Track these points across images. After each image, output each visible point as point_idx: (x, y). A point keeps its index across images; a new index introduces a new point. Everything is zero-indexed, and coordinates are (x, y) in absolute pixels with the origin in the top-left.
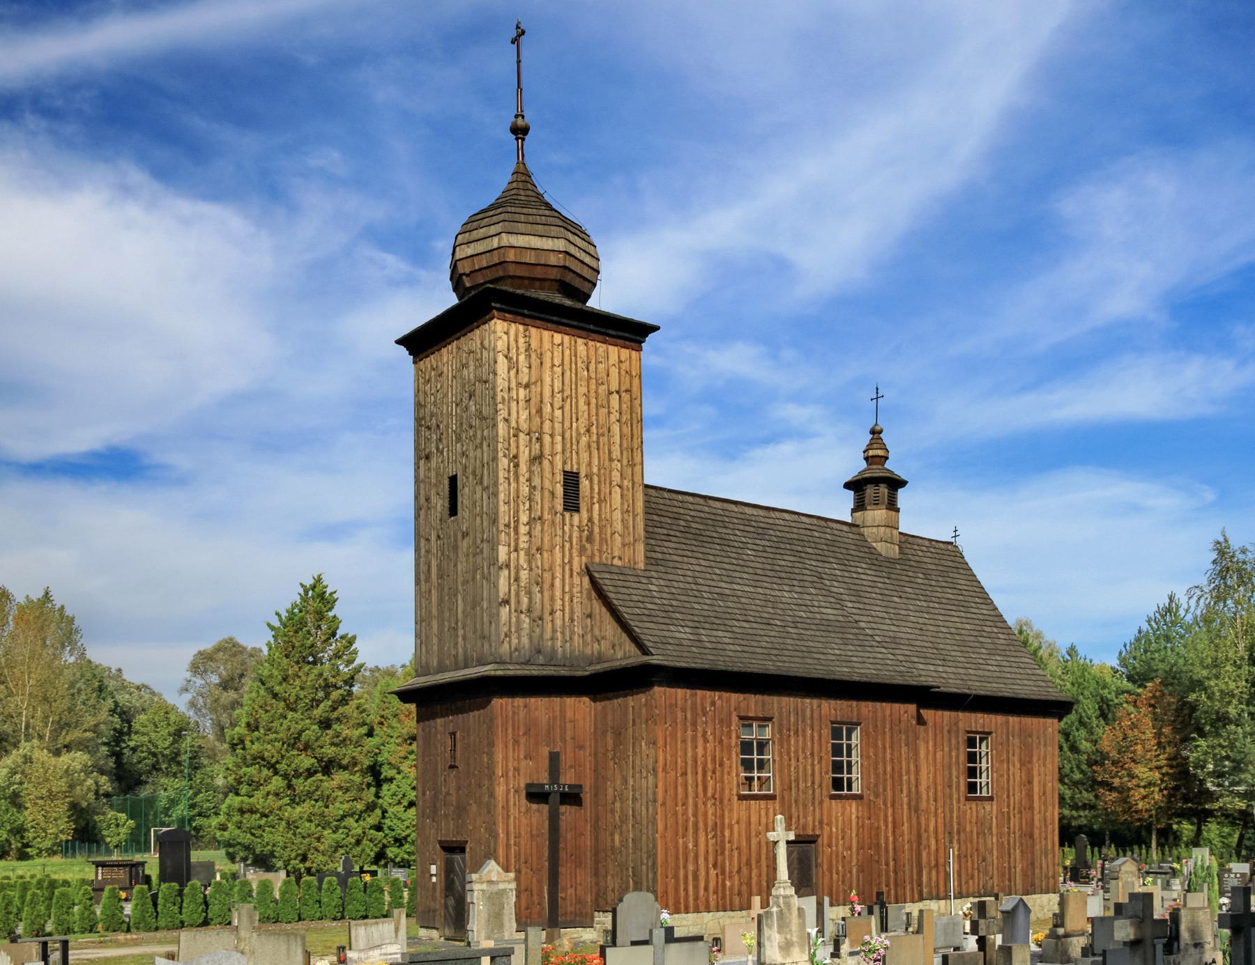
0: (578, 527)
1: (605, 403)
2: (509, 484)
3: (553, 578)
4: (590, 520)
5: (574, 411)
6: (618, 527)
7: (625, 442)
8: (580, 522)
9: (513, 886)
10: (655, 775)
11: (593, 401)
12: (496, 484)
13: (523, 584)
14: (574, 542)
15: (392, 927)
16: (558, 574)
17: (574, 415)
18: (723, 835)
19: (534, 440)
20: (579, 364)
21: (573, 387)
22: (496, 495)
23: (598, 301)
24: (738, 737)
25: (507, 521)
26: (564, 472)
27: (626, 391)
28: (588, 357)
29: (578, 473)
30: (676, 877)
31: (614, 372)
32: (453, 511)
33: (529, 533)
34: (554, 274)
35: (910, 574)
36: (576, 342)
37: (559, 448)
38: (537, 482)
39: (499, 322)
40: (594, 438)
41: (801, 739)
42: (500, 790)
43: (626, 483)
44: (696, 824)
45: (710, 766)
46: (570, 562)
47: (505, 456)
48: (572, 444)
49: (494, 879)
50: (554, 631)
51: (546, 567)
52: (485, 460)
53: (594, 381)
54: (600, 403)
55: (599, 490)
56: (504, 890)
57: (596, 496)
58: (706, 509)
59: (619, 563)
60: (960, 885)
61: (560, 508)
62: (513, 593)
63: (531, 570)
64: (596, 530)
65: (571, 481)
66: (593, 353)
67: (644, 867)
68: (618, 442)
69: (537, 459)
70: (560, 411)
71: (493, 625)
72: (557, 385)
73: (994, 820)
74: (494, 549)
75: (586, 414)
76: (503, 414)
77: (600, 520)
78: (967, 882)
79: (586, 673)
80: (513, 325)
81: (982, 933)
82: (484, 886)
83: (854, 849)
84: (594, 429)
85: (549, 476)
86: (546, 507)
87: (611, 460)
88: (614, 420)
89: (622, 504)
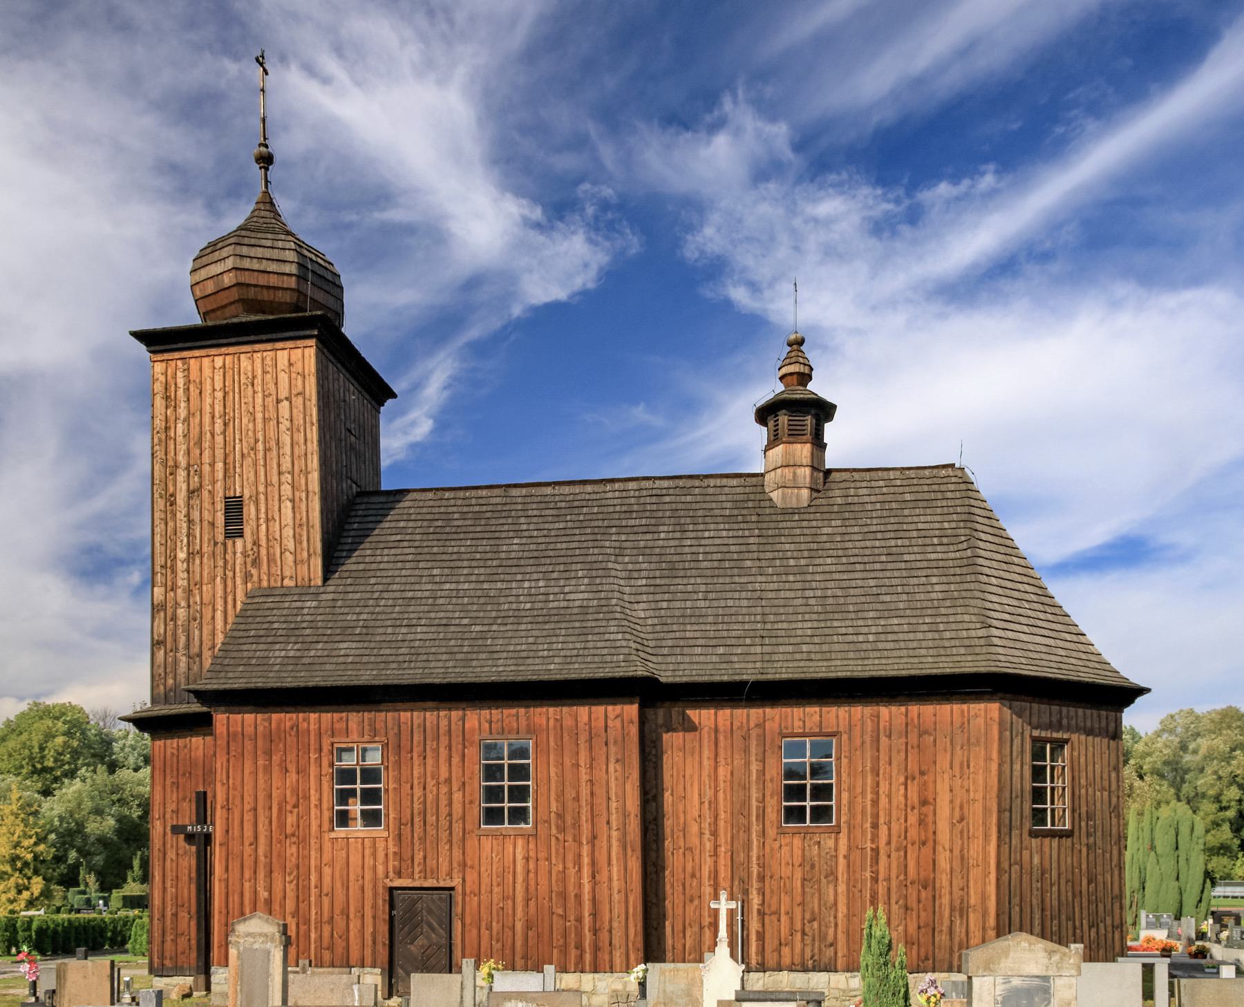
0: (242, 553)
1: (273, 415)
2: (166, 524)
3: (214, 610)
4: (256, 543)
6: (290, 545)
8: (244, 547)
11: (259, 416)
17: (237, 437)
19: (192, 473)
24: (332, 765)
25: (163, 563)
26: (226, 498)
34: (234, 294)
37: (220, 475)
38: (196, 515)
47: (161, 497)
48: (235, 467)
55: (267, 509)
59: (292, 584)
61: (220, 538)
62: (169, 633)
63: (189, 606)
64: (263, 552)
65: (234, 509)
70: (222, 437)
75: (250, 433)
84: (260, 446)
85: (210, 507)
86: (206, 539)
87: (280, 473)
89: (294, 517)
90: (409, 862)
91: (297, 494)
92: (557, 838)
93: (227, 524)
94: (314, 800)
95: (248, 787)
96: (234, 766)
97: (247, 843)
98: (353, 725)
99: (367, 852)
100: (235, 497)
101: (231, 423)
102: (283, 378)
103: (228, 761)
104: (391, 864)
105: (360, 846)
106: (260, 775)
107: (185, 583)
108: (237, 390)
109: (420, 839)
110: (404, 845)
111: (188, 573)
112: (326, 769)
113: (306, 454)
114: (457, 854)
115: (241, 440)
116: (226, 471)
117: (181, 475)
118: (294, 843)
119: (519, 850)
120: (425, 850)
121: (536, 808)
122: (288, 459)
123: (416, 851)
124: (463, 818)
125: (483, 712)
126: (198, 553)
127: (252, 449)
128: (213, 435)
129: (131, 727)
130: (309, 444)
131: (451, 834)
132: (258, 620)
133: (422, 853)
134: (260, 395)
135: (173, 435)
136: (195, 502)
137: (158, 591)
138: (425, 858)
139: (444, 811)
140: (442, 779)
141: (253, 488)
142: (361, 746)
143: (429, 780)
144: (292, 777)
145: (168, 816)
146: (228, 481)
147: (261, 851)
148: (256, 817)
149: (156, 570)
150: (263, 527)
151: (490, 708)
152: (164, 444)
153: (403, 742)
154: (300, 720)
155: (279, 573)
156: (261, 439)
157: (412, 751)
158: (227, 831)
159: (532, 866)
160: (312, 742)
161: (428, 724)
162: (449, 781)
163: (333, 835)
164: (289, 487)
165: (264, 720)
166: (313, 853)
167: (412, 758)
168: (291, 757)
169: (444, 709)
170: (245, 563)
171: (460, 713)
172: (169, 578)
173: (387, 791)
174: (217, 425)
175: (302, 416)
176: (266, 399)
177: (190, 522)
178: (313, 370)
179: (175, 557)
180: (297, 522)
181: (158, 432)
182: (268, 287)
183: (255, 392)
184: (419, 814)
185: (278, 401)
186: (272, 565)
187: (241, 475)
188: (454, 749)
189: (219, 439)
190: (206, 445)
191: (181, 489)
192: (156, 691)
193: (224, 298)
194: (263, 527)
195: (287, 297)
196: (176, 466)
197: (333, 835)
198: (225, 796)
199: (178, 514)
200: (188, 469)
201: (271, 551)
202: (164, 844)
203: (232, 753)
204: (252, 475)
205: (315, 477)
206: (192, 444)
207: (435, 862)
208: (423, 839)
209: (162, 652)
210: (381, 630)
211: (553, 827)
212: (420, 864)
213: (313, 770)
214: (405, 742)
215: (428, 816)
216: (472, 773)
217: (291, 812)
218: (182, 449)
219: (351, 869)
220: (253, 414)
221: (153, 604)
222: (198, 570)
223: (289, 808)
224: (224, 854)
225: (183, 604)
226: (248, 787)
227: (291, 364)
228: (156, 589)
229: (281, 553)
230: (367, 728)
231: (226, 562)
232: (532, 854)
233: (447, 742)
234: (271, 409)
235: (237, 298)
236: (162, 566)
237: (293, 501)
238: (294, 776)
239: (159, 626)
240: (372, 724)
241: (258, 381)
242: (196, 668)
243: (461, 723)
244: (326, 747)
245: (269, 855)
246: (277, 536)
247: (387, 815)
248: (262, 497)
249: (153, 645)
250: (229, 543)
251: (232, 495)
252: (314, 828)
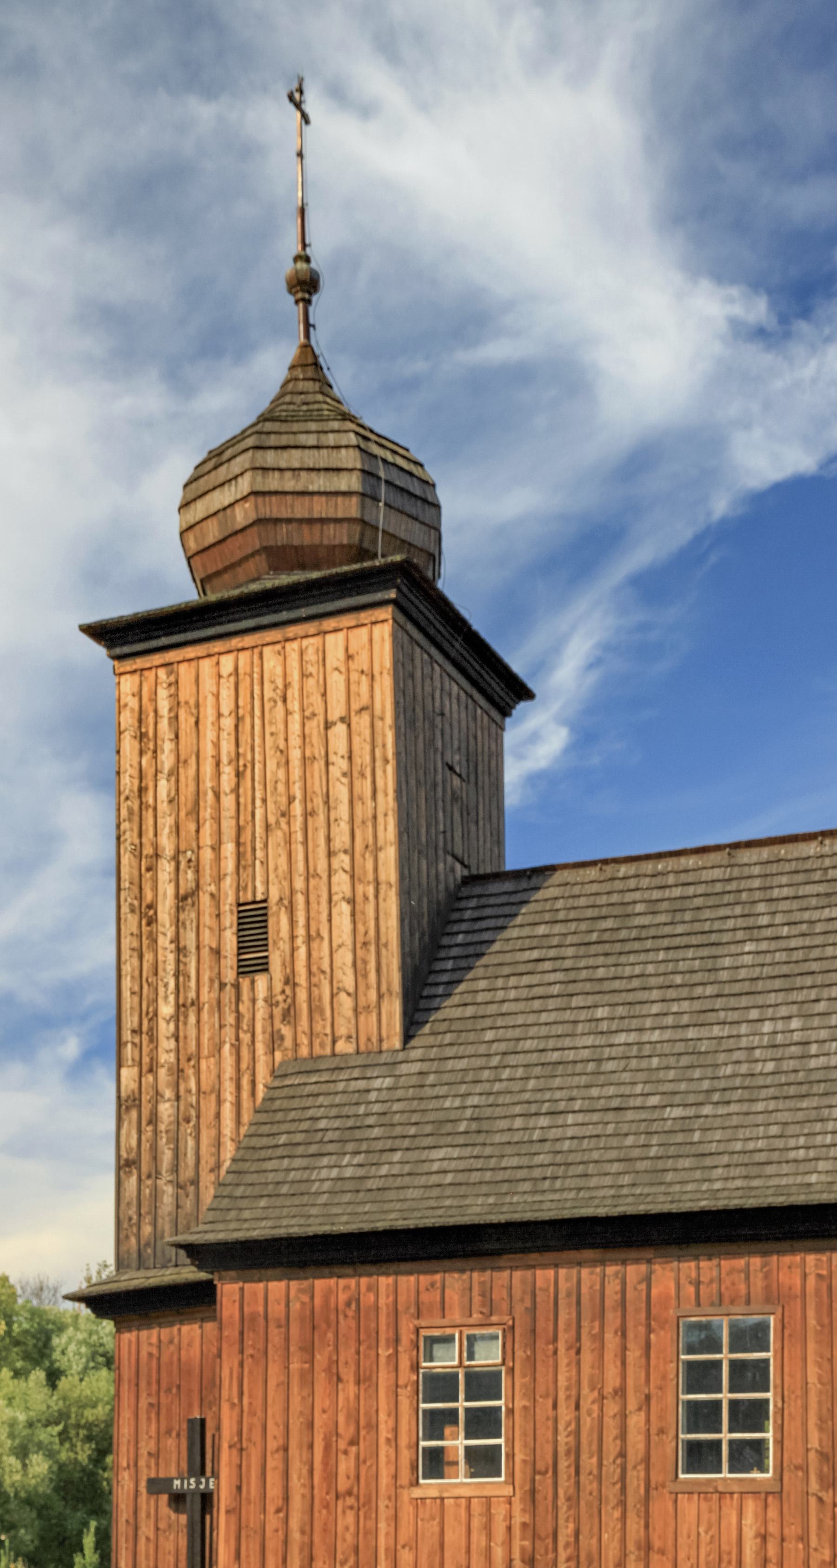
0: (266, 1000)
1: (318, 750)
7: (358, 809)
8: (270, 988)
11: (295, 755)
17: (258, 795)
20: (268, 693)
28: (285, 675)
37: (229, 865)
40: (298, 824)
48: (254, 850)
54: (308, 754)
64: (302, 995)
75: (281, 787)
84: (297, 808)
87: (330, 854)
90: (550, 1541)
91: (360, 889)
92: (820, 1500)
93: (241, 949)
94: (384, 1432)
95: (275, 1410)
96: (250, 1372)
97: (271, 1509)
98: (453, 1296)
99: (476, 1523)
100: (254, 902)
102: (336, 682)
103: (241, 1364)
104: (517, 1544)
105: (463, 1512)
106: (295, 1389)
107: (172, 1058)
109: (568, 1499)
110: (540, 1509)
111: (177, 1040)
112: (406, 1375)
113: (375, 817)
114: (634, 1526)
115: (264, 801)
116: (239, 856)
117: (166, 869)
118: (351, 1508)
119: (749, 1520)
120: (577, 1521)
121: (780, 1442)
122: (344, 827)
123: (561, 1522)
124: (647, 1460)
125: (684, 1266)
126: (193, 1004)
127: (283, 815)
128: (217, 796)
129: (84, 1311)
130: (380, 796)
131: (623, 1489)
132: (292, 1115)
133: (571, 1526)
134: (296, 718)
135: (151, 801)
136: (189, 915)
137: (128, 1074)
138: (577, 1533)
139: (611, 1447)
140: (608, 1389)
141: (286, 884)
142: (467, 1332)
143: (585, 1391)
144: (349, 1389)
145: (142, 1463)
146: (243, 875)
147: (295, 1523)
148: (286, 1462)
149: (124, 1039)
150: (302, 952)
151: (696, 1258)
152: (136, 818)
153: (540, 1324)
154: (363, 1289)
155: (328, 1031)
157: (555, 1339)
158: (239, 1488)
159: (772, 1550)
160: (383, 1328)
161: (584, 1290)
162: (621, 1392)
163: (417, 1493)
164: (346, 878)
165: (301, 1291)
166: (382, 1525)
167: (555, 1352)
168: (347, 1354)
169: (614, 1262)
170: (271, 1017)
171: (643, 1268)
172: (145, 1050)
173: (511, 1412)
174: (224, 778)
175: (368, 748)
176: (308, 724)
177: (180, 950)
178: (388, 663)
179: (156, 1014)
180: (360, 939)
181: (127, 798)
182: (310, 521)
183: (288, 713)
184: (568, 1453)
185: (328, 725)
186: (317, 1017)
187: (265, 863)
188: (630, 1335)
189: (228, 802)
190: (206, 813)
191: (165, 894)
192: (124, 1248)
193: (235, 549)
194: (302, 952)
195: (341, 536)
196: (157, 856)
197: (417, 1493)
198: (235, 1429)
200: (176, 859)
201: (315, 991)
202: (136, 1512)
203: (249, 1351)
204: (283, 862)
205: (390, 856)
206: (182, 814)
207: (594, 1541)
208: (574, 1500)
209: (134, 1180)
210: (503, 1124)
211: (813, 1478)
212: (567, 1545)
213: (384, 1378)
214: (544, 1325)
215: (584, 1457)
216: (664, 1377)
217: (346, 1452)
218: (166, 823)
219: (447, 1554)
220: (284, 753)
221: (119, 1097)
222: (192, 1032)
223: (342, 1445)
224: (233, 1527)
225: (168, 1093)
226: (275, 1410)
227: (349, 657)
228: (124, 1072)
229: (332, 996)
230: (477, 1299)
232: (773, 1528)
233: (618, 1322)
234: (316, 739)
235: (257, 546)
236: (134, 1031)
237: (352, 901)
238: (352, 1389)
239: (128, 1135)
240: (487, 1294)
242: (188, 1204)
243: (643, 1286)
244: (406, 1336)
245: (308, 1529)
246: (326, 966)
247: (511, 1456)
248: (300, 899)
249: (119, 1168)
250: (245, 983)
251: (250, 898)
252: (385, 1480)
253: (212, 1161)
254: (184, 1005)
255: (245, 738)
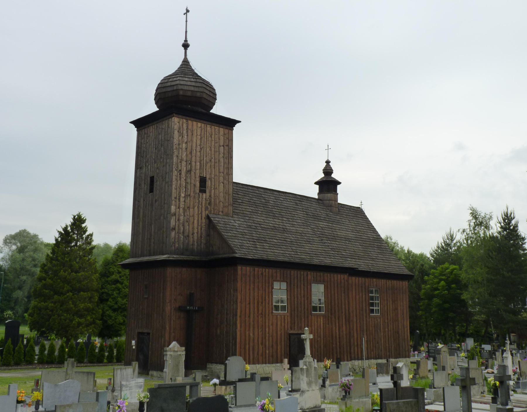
1: (217, 150)
2: (177, 181)
3: (194, 219)
4: (210, 196)
5: (205, 153)
9: (184, 353)
10: (237, 304)
11: (213, 149)
12: (172, 181)
13: (181, 222)
14: (203, 205)
15: (132, 370)
16: (196, 218)
17: (205, 155)
18: (265, 331)
19: (188, 164)
21: (205, 143)
22: (171, 185)
23: (216, 110)
26: (200, 177)
27: (227, 145)
29: (206, 178)
30: (245, 349)
31: (222, 138)
32: (151, 190)
33: (185, 201)
35: (343, 220)
36: (206, 126)
37: (198, 167)
38: (189, 180)
39: (175, 118)
41: (299, 289)
42: (168, 308)
43: (225, 182)
44: (254, 325)
45: (260, 300)
46: (201, 213)
48: (204, 166)
49: (176, 350)
50: (193, 241)
51: (191, 215)
52: (167, 171)
53: (214, 141)
54: (216, 150)
56: (180, 355)
57: (213, 186)
58: (257, 192)
60: (368, 353)
61: (198, 191)
62: (177, 225)
63: (184, 216)
64: (213, 200)
65: (203, 181)
66: (214, 131)
67: (231, 344)
68: (223, 166)
69: (189, 171)
71: (168, 239)
72: (198, 142)
73: (382, 325)
74: (169, 207)
75: (210, 154)
76: (176, 153)
77: (214, 196)
78: (371, 353)
79: (207, 259)
80: (181, 119)
81: (395, 380)
82: (172, 353)
83: (322, 337)
87: (220, 172)
88: (221, 156)
93: (200, 186)
100: (203, 177)
101: (203, 149)
108: (205, 137)
111: (185, 202)
116: (200, 166)
117: (184, 163)
135: (181, 147)
156: (213, 157)
164: (222, 178)
177: (186, 183)
199: (182, 179)
204: (210, 170)
231: (199, 201)
241: (213, 136)
253: (192, 232)
254: (187, 195)
255: (203, 141)
